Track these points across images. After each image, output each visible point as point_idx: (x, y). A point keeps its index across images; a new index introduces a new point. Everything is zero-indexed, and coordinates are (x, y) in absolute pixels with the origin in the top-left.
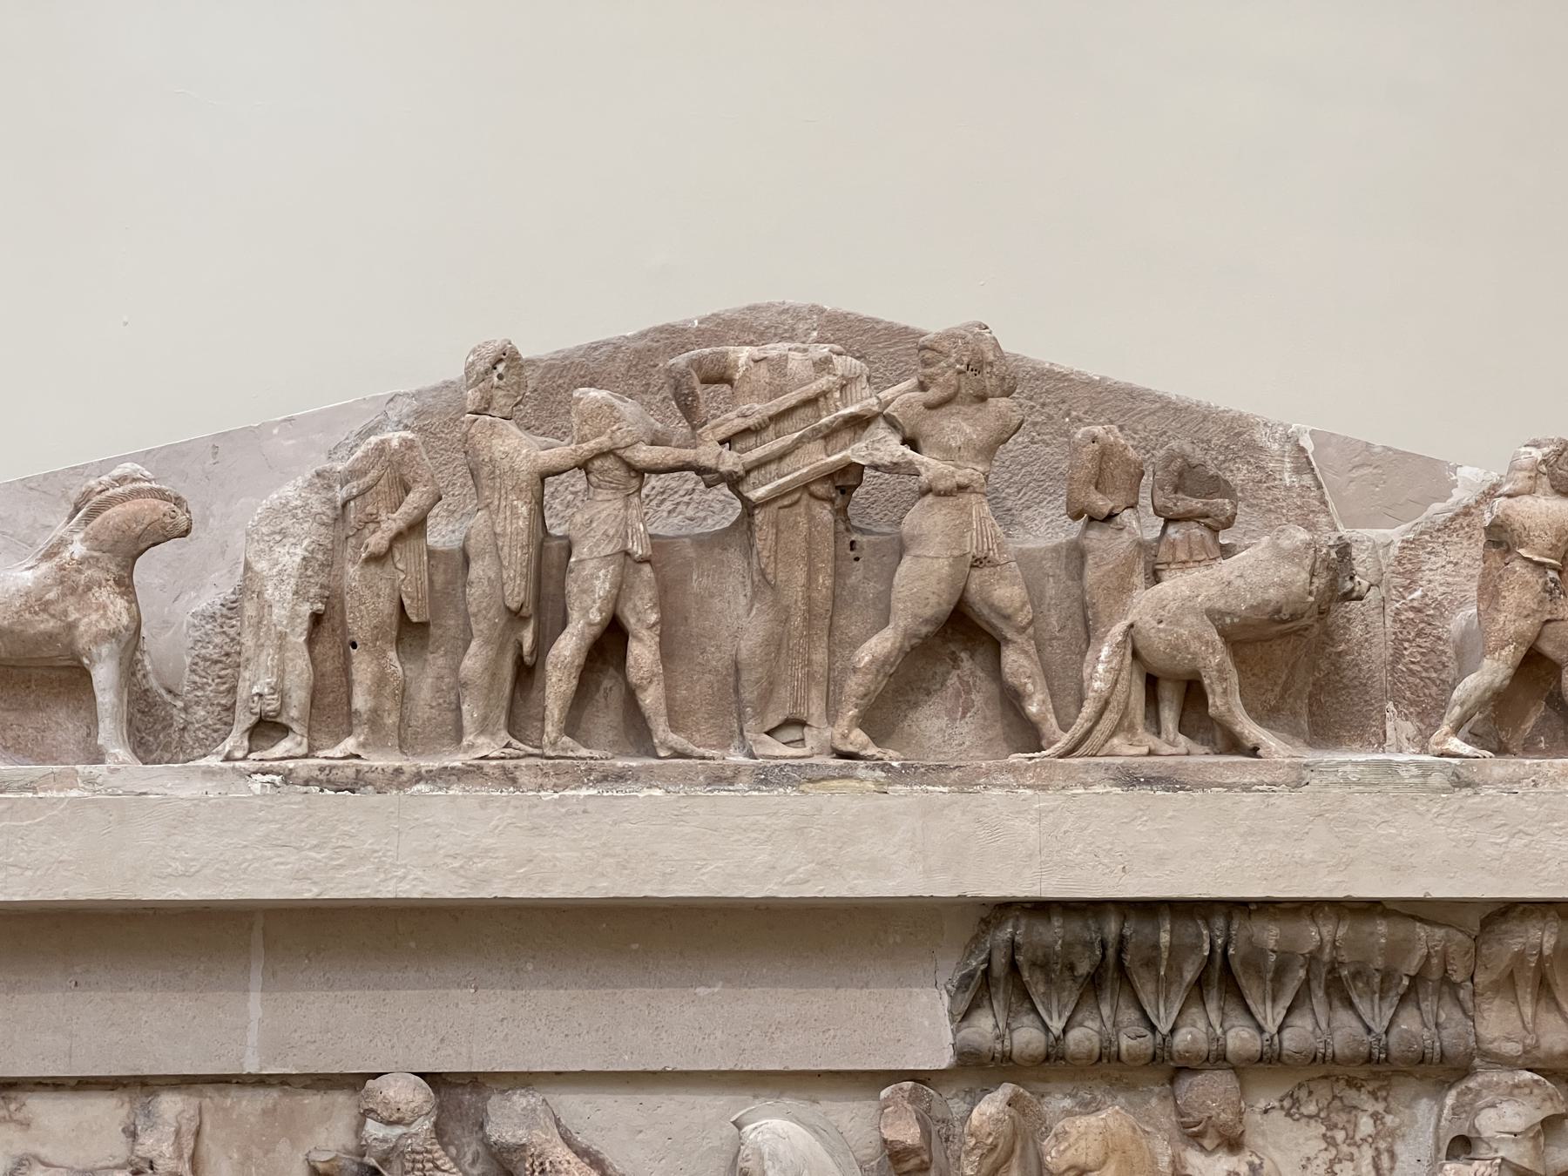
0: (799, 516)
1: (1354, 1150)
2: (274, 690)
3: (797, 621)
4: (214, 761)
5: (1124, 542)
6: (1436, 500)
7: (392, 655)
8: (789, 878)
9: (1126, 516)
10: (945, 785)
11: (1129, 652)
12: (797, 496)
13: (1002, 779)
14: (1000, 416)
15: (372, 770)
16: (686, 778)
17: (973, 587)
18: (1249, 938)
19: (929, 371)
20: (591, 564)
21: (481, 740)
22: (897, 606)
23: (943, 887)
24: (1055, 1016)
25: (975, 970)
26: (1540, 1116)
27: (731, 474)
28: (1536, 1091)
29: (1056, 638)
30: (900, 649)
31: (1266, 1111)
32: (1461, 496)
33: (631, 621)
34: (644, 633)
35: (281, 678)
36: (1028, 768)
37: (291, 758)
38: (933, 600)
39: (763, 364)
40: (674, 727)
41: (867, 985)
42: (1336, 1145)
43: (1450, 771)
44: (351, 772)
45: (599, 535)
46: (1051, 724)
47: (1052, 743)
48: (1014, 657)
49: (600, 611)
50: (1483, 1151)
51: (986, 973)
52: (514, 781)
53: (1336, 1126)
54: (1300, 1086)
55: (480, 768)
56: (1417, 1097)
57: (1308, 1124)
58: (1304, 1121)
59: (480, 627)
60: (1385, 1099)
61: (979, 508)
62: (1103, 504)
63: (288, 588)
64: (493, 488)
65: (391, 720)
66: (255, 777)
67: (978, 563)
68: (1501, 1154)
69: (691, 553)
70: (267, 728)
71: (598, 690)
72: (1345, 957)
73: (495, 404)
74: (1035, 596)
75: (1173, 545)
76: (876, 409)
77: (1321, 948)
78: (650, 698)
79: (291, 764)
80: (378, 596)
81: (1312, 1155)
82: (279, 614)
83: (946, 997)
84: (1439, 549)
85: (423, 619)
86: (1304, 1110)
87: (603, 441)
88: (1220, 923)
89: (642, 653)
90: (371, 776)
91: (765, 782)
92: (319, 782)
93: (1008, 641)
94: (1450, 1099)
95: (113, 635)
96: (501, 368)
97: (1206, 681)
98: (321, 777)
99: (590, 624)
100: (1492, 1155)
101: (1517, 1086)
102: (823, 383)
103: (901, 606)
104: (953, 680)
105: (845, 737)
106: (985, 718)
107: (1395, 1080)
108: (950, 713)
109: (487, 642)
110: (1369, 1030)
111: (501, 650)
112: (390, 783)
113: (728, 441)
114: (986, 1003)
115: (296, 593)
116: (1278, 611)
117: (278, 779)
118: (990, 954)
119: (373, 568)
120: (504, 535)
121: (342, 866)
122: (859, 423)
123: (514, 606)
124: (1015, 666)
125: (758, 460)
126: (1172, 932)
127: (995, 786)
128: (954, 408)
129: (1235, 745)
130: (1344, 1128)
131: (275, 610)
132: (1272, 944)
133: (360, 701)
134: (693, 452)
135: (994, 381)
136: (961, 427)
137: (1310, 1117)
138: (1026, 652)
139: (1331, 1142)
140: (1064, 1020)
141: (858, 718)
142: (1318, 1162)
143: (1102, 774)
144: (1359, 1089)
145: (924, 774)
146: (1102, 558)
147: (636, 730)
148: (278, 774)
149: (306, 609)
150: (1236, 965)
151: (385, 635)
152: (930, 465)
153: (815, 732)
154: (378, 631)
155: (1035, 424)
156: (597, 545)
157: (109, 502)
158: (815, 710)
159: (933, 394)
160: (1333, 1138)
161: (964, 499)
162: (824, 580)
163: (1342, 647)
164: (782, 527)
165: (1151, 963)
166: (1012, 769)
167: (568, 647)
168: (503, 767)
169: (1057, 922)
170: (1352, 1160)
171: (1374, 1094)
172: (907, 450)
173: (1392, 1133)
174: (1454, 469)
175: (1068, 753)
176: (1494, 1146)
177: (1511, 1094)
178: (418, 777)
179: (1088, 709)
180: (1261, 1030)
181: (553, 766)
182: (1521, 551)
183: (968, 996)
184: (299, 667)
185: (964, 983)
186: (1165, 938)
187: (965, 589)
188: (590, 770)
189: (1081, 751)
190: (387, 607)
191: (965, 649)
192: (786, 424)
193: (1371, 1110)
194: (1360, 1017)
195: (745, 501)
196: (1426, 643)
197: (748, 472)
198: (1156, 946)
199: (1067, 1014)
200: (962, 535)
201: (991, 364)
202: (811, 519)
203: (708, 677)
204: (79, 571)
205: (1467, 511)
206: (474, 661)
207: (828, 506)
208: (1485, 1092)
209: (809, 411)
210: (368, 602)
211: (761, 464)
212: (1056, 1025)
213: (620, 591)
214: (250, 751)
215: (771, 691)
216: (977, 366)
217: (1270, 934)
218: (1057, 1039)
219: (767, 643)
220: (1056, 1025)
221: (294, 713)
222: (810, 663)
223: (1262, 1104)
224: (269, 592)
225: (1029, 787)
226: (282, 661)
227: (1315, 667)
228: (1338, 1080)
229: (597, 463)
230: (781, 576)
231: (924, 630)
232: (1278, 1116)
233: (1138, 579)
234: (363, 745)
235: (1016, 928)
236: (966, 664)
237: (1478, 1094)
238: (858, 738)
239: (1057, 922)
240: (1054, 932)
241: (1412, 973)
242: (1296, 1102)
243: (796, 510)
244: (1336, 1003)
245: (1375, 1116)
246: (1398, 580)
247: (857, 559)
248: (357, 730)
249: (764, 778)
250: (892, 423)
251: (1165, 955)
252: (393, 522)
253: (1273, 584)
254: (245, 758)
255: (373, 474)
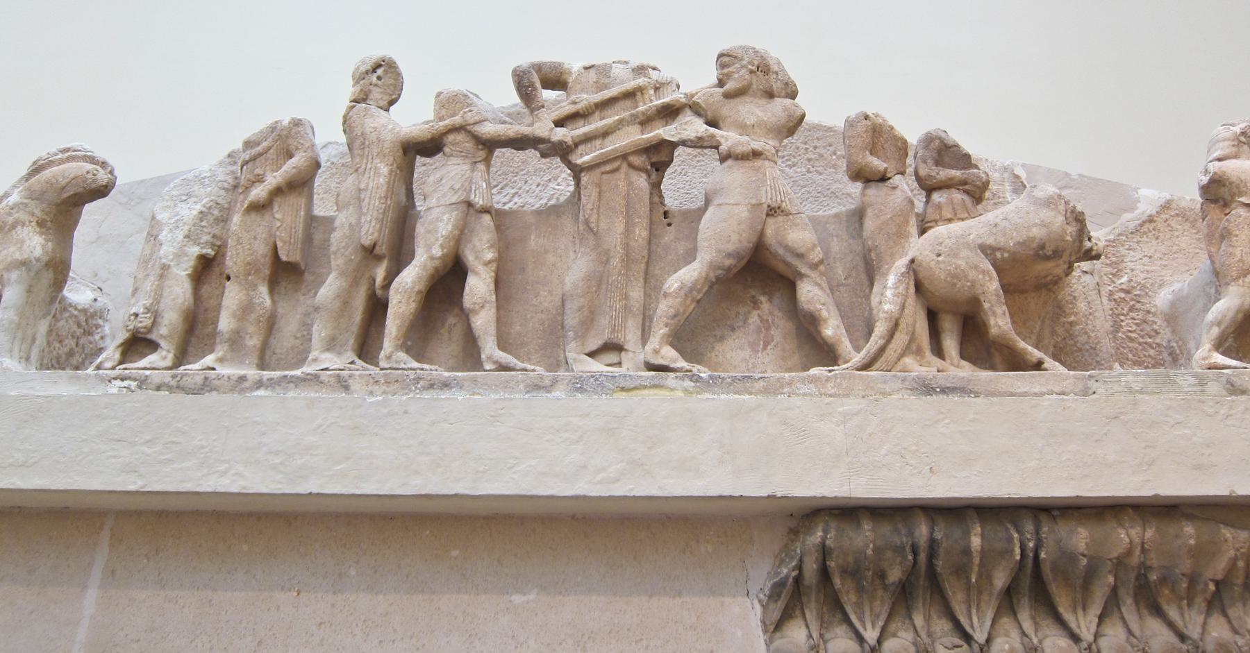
0: (620, 179)
2: (148, 310)
3: (616, 262)
4: (90, 371)
5: (897, 199)
6: (1126, 211)
7: (264, 290)
8: (599, 477)
9: (897, 180)
10: (750, 394)
11: (912, 283)
12: (616, 164)
13: (805, 388)
14: (786, 109)
15: (219, 378)
16: (506, 386)
17: (769, 232)
18: (1058, 542)
19: (726, 71)
20: (438, 210)
21: (327, 355)
22: (702, 243)
23: (753, 485)
24: (869, 625)
25: (787, 577)
27: (561, 143)
29: (842, 285)
30: (707, 278)
32: (1146, 207)
33: (470, 258)
34: (481, 269)
35: (158, 298)
36: (828, 379)
37: (154, 369)
38: (735, 238)
39: (592, 72)
40: (503, 344)
41: (679, 594)
43: (1224, 380)
44: (199, 379)
45: (447, 187)
46: (845, 346)
47: (846, 362)
48: (809, 288)
49: (442, 246)
51: (798, 580)
52: (346, 388)
55: (317, 376)
59: (337, 262)
61: (770, 171)
62: (878, 164)
63: (180, 235)
64: (362, 156)
65: (253, 342)
66: (114, 382)
67: (773, 211)
69: (531, 219)
70: (138, 344)
71: (443, 325)
72: (1154, 560)
73: (371, 96)
74: (823, 242)
75: (939, 207)
76: (683, 100)
77: (1129, 552)
78: (483, 322)
79: (148, 372)
80: (255, 238)
82: (167, 251)
83: (758, 608)
84: (1135, 246)
85: (292, 259)
87: (457, 120)
88: (1029, 527)
89: (478, 286)
90: (215, 382)
91: (581, 390)
92: (170, 388)
93: (801, 276)
95: (24, 264)
96: (380, 72)
97: (986, 306)
98: (173, 383)
99: (432, 258)
102: (641, 81)
103: (706, 244)
104: (754, 318)
105: (656, 352)
106: (784, 350)
108: (753, 346)
109: (342, 274)
110: (1183, 637)
111: (355, 283)
112: (232, 389)
113: (559, 123)
114: (798, 612)
115: (187, 236)
116: (1042, 247)
117: (133, 384)
118: (801, 561)
119: (253, 215)
120: (365, 190)
121: (169, 460)
122: (670, 112)
123: (367, 242)
124: (811, 295)
125: (585, 134)
126: (983, 536)
127: (798, 395)
128: (747, 99)
129: (1017, 363)
131: (164, 247)
132: (1082, 547)
133: (225, 323)
134: (530, 129)
135: (779, 84)
136: (753, 110)
138: (819, 285)
140: (878, 630)
141: (669, 336)
143: (899, 384)
145: (730, 384)
146: (881, 210)
147: (470, 355)
148: (135, 380)
149: (195, 251)
150: (1046, 570)
151: (258, 271)
152: (728, 138)
153: (631, 355)
154: (251, 267)
155: (809, 160)
156: (444, 196)
157: (49, 164)
158: (630, 337)
159: (730, 86)
161: (758, 163)
162: (641, 232)
163: (1072, 318)
164: (604, 188)
165: (961, 570)
166: (814, 380)
167: (412, 277)
168: (338, 376)
169: (867, 526)
172: (712, 130)
174: (1136, 190)
175: (866, 367)
178: (260, 384)
179: (880, 329)
180: (1075, 638)
181: (385, 375)
182: (1244, 200)
183: (781, 604)
184: (180, 290)
185: (776, 592)
186: (976, 542)
187: (762, 234)
188: (418, 379)
189: (877, 365)
190: (261, 249)
191: (764, 294)
192: (609, 112)
194: (1171, 625)
195: (570, 165)
196: (1140, 315)
197: (576, 145)
198: (967, 551)
199: (881, 623)
200: (758, 189)
201: (776, 73)
202: (630, 184)
203: (539, 316)
204: (10, 214)
205: (1151, 220)
206: (329, 289)
207: (644, 176)
209: (628, 103)
210: (247, 243)
211: (587, 139)
212: (871, 635)
213: (461, 236)
214: (121, 363)
215: (592, 320)
216: (763, 68)
217: (1080, 538)
218: (873, 649)
219: (588, 278)
220: (871, 635)
221: (164, 331)
222: (627, 297)
224: (164, 235)
225: (831, 396)
226: (161, 287)
227: (1053, 333)
229: (451, 137)
230: (603, 226)
231: (728, 262)
233: (913, 229)
234: (221, 360)
235: (825, 531)
236: (765, 305)
238: (669, 355)
239: (867, 526)
240: (865, 536)
241: (1219, 576)
243: (617, 175)
244: (1145, 612)
246: (1109, 269)
247: (669, 225)
248: (218, 348)
249: (579, 386)
250: (696, 109)
251: (976, 561)
252: (273, 179)
253: (1036, 225)
254: (113, 368)
255: (265, 144)
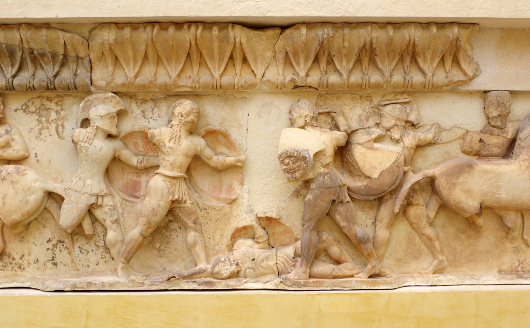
1: (49, 125)
26: (115, 110)
28: (113, 100)
31: (16, 110)
42: (42, 123)
50: (92, 124)
53: (42, 116)
54: (29, 101)
56: (72, 105)
57: (32, 115)
58: (30, 114)
60: (61, 105)
68: (96, 124)
81: (33, 127)
86: (30, 110)
94: (82, 105)
100: (93, 125)
101: (106, 98)
107: (65, 98)
130: (45, 117)
137: (32, 112)
139: (40, 122)
142: (35, 129)
144: (51, 102)
160: (41, 120)
170: (48, 129)
171: (56, 103)
173: (63, 118)
176: (94, 121)
177: (104, 102)
193: (55, 110)
208: (95, 101)
223: (14, 108)
228: (43, 98)
232: (20, 112)
237: (92, 102)
242: (27, 107)
245: (57, 112)
